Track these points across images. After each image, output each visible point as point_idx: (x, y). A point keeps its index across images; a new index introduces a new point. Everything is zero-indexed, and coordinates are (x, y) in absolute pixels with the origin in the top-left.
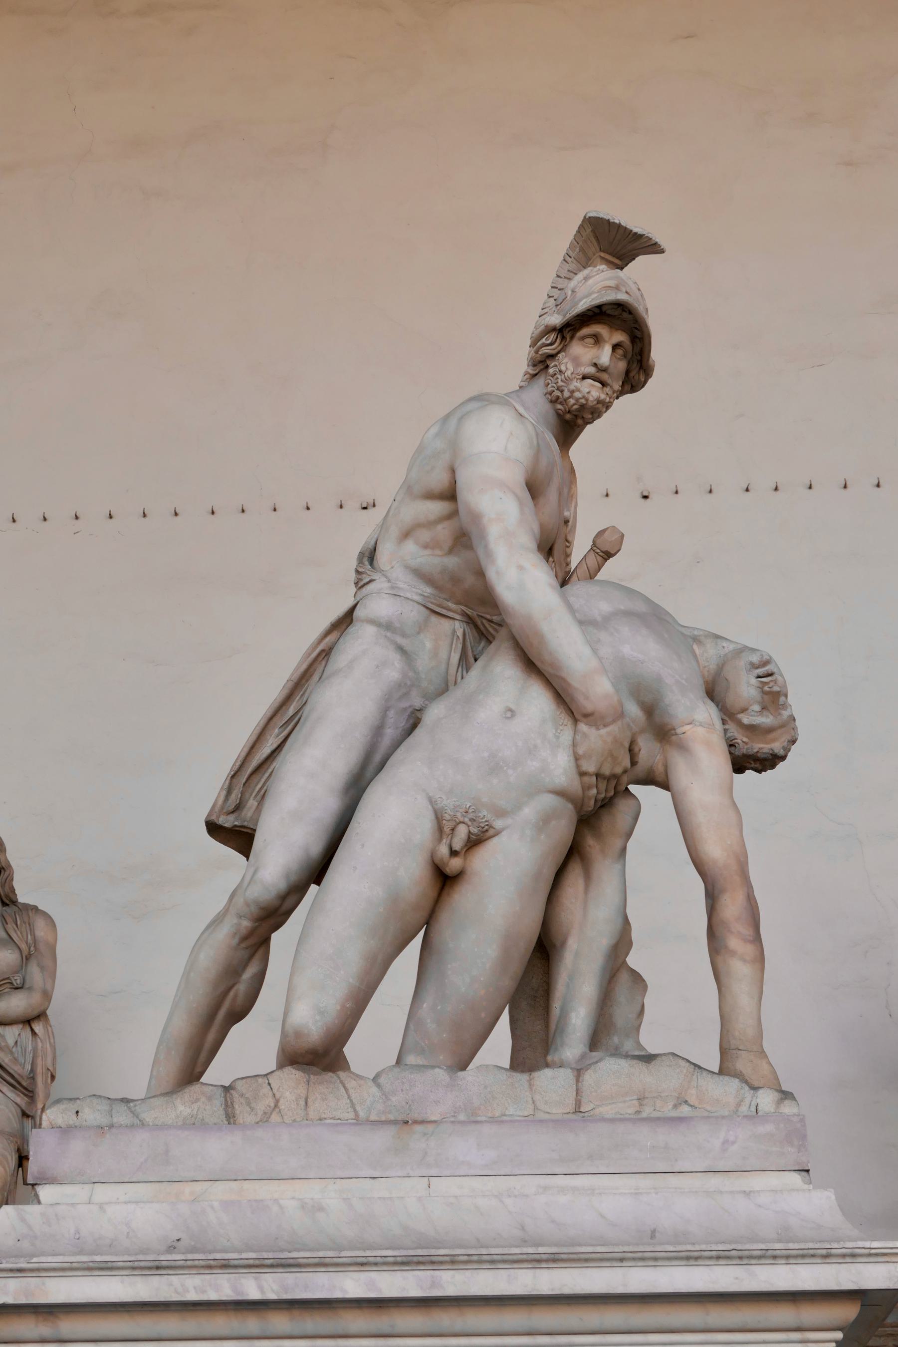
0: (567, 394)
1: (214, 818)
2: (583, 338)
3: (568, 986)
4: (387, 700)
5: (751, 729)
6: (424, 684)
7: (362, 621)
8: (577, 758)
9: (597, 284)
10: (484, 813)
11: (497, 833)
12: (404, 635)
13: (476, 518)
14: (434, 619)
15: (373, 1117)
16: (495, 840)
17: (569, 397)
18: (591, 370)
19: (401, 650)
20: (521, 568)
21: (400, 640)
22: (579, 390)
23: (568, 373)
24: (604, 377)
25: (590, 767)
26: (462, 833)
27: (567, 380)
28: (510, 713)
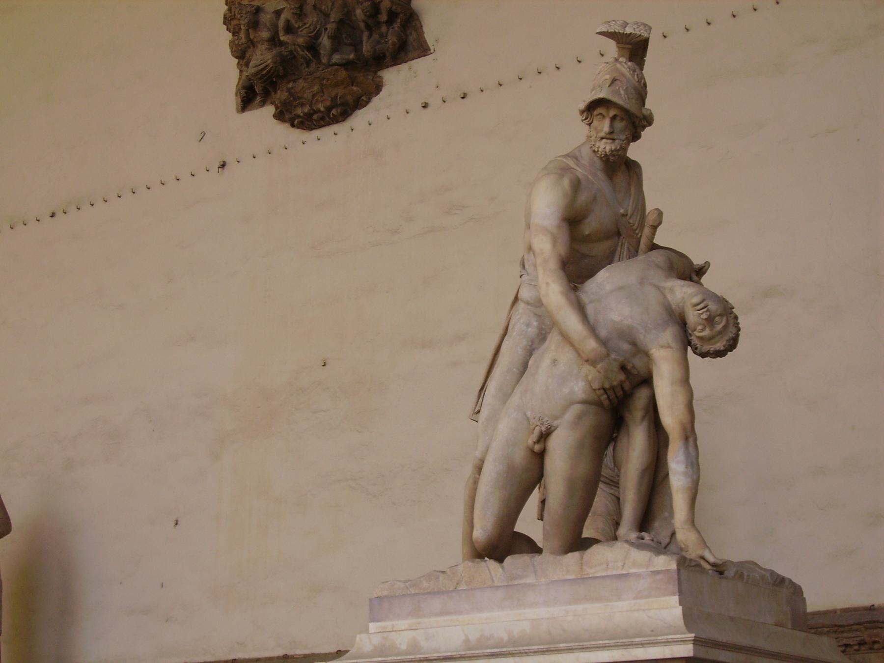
4: (531, 346)
5: (701, 338)
11: (556, 429)
19: (535, 314)
20: (547, 283)
24: (611, 136)
25: (596, 386)
28: (555, 362)
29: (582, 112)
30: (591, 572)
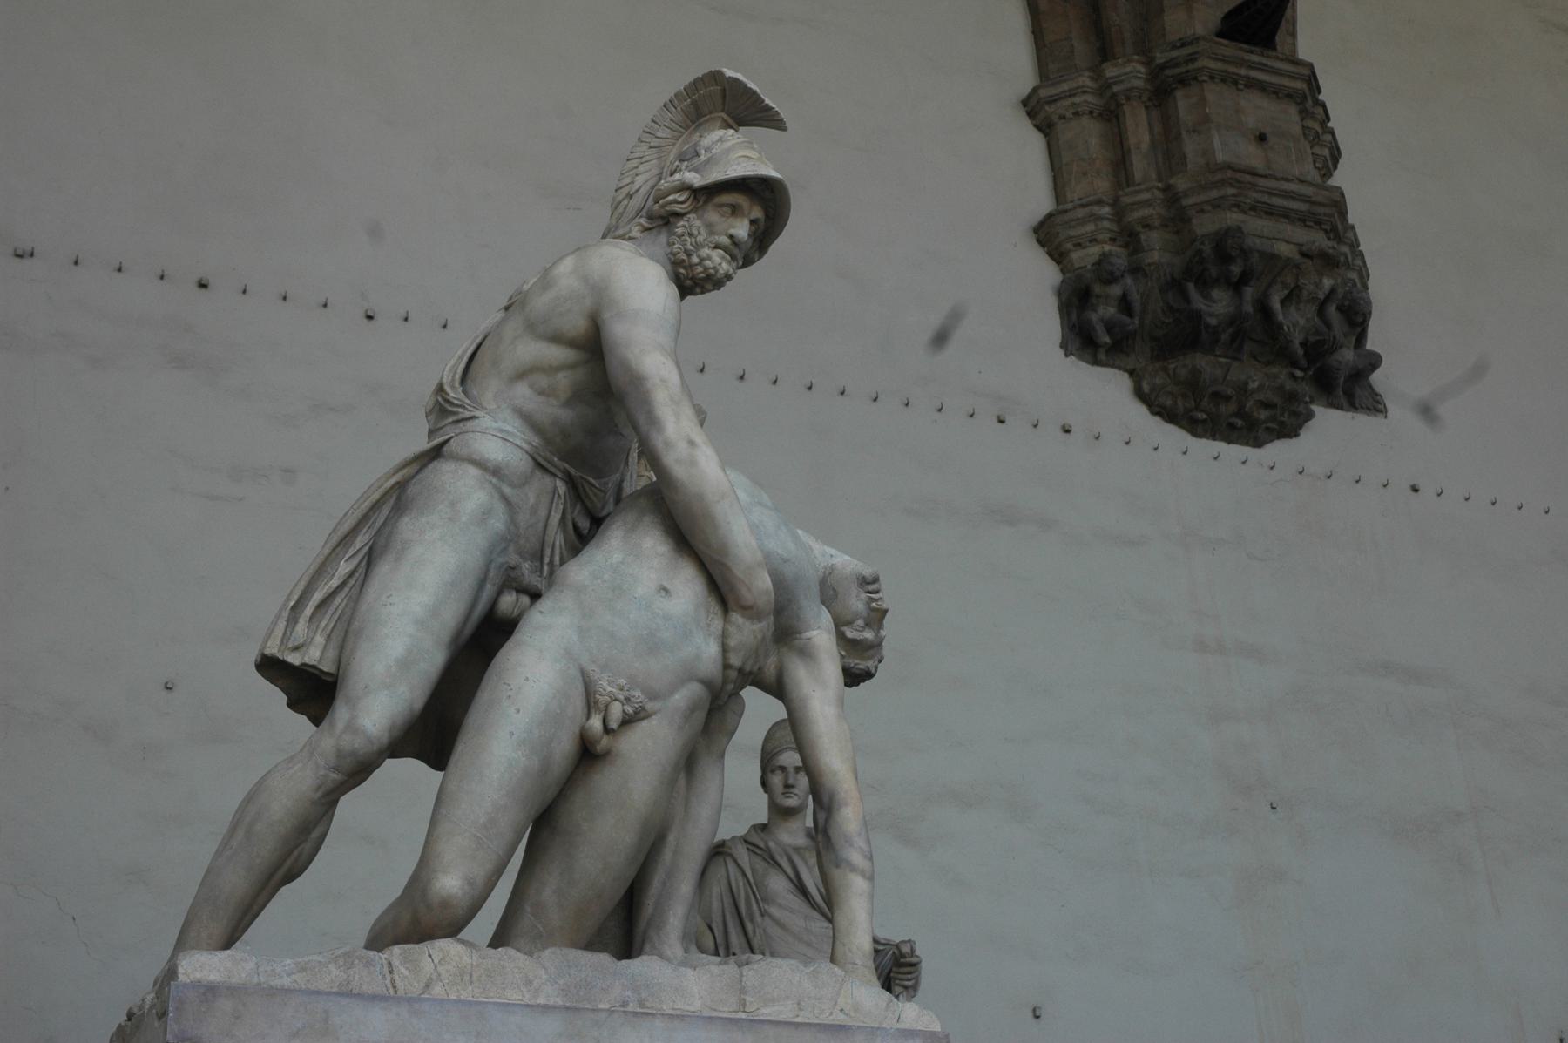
0: (695, 260)
1: (273, 649)
2: (721, 205)
3: (664, 883)
6: (522, 542)
7: (456, 458)
8: (725, 649)
9: (735, 154)
10: (637, 693)
11: (648, 716)
12: (512, 485)
13: (638, 380)
14: (538, 473)
15: (541, 1001)
16: (644, 723)
17: (699, 264)
18: (725, 240)
20: (692, 443)
21: (507, 490)
22: (709, 258)
23: (700, 239)
24: (736, 251)
25: (735, 660)
26: (616, 711)
27: (698, 246)
29: (685, 187)
30: (767, 1012)
